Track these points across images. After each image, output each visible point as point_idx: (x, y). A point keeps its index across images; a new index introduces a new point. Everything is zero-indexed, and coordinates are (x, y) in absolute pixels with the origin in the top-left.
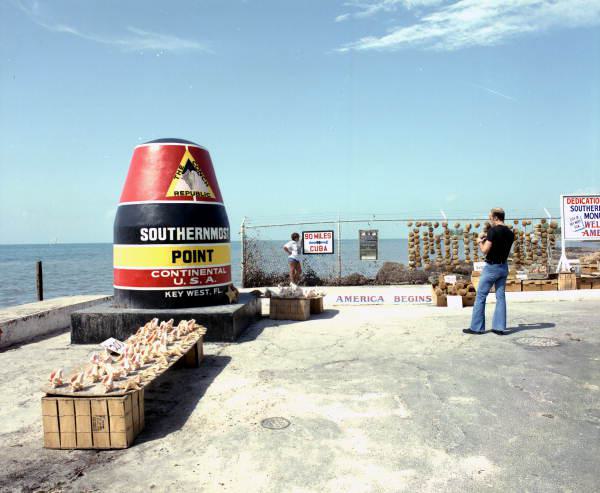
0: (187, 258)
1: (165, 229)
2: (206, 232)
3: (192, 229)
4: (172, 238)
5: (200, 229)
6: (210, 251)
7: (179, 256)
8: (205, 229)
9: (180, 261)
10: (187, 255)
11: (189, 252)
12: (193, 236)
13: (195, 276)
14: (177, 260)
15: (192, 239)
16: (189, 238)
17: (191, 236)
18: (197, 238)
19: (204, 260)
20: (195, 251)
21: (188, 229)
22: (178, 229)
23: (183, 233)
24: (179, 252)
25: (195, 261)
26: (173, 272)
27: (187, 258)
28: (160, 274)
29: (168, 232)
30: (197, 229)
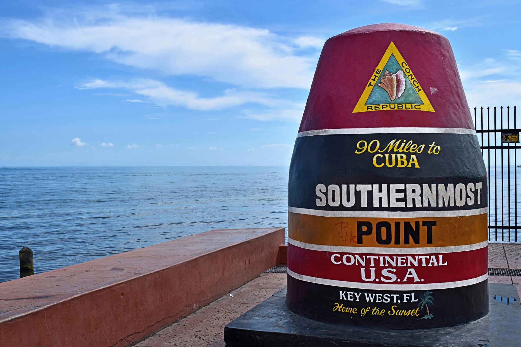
13: (390, 266)
26: (358, 257)
28: (340, 259)
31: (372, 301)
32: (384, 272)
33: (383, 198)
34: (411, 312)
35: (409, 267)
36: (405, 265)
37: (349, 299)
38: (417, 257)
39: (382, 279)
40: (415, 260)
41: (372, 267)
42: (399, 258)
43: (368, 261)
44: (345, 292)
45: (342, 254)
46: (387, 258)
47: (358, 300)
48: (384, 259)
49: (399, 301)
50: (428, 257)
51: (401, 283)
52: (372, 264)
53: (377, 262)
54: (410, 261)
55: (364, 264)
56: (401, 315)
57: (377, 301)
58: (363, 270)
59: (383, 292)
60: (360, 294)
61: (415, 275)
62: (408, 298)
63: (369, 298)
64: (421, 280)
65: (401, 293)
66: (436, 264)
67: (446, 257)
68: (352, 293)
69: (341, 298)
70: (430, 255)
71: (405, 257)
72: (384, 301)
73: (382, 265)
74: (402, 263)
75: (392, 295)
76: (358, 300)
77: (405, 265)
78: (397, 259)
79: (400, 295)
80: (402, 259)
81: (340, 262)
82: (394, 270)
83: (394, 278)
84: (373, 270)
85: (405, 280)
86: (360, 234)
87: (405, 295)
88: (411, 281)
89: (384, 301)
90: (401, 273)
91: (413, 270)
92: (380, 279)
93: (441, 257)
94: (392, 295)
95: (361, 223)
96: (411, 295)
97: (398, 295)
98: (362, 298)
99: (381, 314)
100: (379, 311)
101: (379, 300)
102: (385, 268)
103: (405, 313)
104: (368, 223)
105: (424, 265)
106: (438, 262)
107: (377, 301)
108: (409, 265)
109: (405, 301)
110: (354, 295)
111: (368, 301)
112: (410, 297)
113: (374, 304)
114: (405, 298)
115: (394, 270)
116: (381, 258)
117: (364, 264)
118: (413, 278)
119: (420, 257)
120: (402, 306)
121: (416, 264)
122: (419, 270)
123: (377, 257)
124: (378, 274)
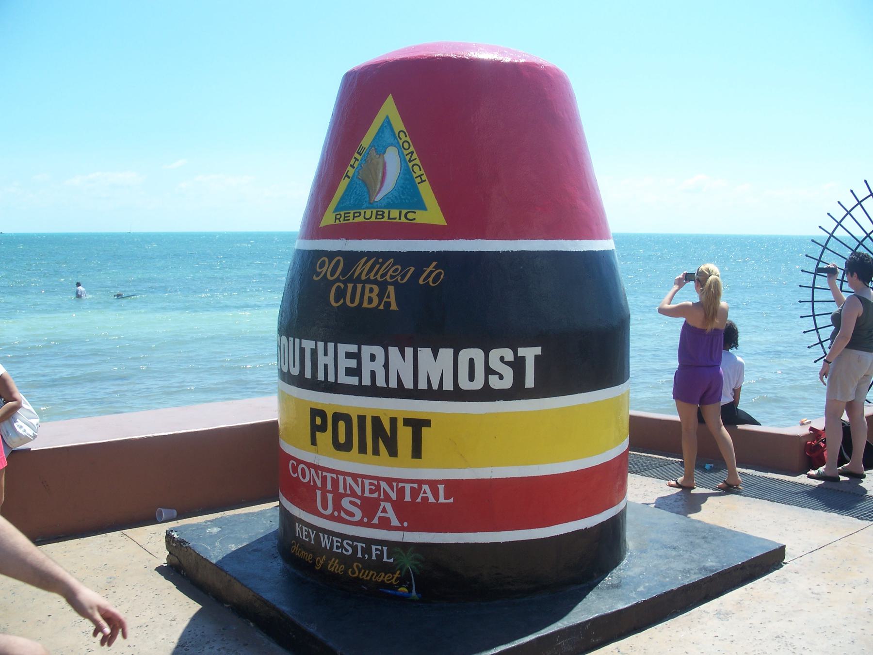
0: (342, 439)
1: (297, 340)
3: (353, 348)
4: (308, 375)
5: (378, 351)
6: (417, 425)
7: (323, 428)
8: (394, 351)
9: (325, 438)
10: (342, 425)
11: (347, 418)
13: (353, 494)
14: (318, 434)
15: (353, 381)
16: (343, 379)
17: (349, 372)
18: (366, 381)
19: (393, 452)
21: (343, 348)
23: (330, 360)
24: (322, 414)
25: (363, 450)
27: (342, 439)
29: (302, 350)
31: (328, 548)
32: (345, 503)
34: (384, 577)
35: (384, 500)
36: (375, 495)
37: (304, 538)
38: (395, 484)
39: (343, 514)
40: (393, 490)
41: (329, 492)
42: (367, 482)
43: (324, 479)
44: (300, 526)
45: (300, 462)
46: (349, 480)
47: (313, 542)
48: (345, 480)
49: (366, 556)
50: (416, 486)
51: (369, 525)
52: (329, 487)
53: (335, 482)
55: (319, 484)
56: (368, 578)
57: (335, 550)
58: (319, 493)
59: (343, 537)
60: (315, 532)
61: (391, 514)
62: (379, 553)
63: (325, 542)
64: (402, 524)
65: (369, 542)
66: (432, 500)
67: (452, 486)
68: (307, 529)
69: (297, 535)
70: (420, 482)
71: (375, 482)
72: (344, 551)
73: (341, 490)
74: (371, 491)
75: (355, 544)
76: (313, 542)
77: (375, 495)
78: (363, 483)
80: (370, 484)
81: (295, 475)
82: (359, 502)
83: (358, 515)
84: (330, 497)
85: (375, 521)
86: (315, 429)
87: (374, 547)
88: (385, 524)
89: (344, 551)
90: (369, 507)
91: (388, 506)
92: (339, 513)
93: (441, 488)
94: (355, 544)
95: (316, 412)
96: (382, 548)
97: (364, 545)
98: (317, 537)
100: (338, 565)
101: (338, 547)
102: (345, 495)
103: (374, 577)
105: (408, 498)
106: (436, 497)
107: (335, 550)
108: (382, 497)
109: (374, 558)
111: (323, 546)
112: (382, 551)
113: (330, 553)
114: (374, 553)
115: (359, 502)
116: (341, 478)
117: (319, 484)
118: (388, 520)
119: (400, 485)
120: (368, 565)
121: (393, 496)
122: (399, 506)
123: (334, 476)
124: (337, 506)
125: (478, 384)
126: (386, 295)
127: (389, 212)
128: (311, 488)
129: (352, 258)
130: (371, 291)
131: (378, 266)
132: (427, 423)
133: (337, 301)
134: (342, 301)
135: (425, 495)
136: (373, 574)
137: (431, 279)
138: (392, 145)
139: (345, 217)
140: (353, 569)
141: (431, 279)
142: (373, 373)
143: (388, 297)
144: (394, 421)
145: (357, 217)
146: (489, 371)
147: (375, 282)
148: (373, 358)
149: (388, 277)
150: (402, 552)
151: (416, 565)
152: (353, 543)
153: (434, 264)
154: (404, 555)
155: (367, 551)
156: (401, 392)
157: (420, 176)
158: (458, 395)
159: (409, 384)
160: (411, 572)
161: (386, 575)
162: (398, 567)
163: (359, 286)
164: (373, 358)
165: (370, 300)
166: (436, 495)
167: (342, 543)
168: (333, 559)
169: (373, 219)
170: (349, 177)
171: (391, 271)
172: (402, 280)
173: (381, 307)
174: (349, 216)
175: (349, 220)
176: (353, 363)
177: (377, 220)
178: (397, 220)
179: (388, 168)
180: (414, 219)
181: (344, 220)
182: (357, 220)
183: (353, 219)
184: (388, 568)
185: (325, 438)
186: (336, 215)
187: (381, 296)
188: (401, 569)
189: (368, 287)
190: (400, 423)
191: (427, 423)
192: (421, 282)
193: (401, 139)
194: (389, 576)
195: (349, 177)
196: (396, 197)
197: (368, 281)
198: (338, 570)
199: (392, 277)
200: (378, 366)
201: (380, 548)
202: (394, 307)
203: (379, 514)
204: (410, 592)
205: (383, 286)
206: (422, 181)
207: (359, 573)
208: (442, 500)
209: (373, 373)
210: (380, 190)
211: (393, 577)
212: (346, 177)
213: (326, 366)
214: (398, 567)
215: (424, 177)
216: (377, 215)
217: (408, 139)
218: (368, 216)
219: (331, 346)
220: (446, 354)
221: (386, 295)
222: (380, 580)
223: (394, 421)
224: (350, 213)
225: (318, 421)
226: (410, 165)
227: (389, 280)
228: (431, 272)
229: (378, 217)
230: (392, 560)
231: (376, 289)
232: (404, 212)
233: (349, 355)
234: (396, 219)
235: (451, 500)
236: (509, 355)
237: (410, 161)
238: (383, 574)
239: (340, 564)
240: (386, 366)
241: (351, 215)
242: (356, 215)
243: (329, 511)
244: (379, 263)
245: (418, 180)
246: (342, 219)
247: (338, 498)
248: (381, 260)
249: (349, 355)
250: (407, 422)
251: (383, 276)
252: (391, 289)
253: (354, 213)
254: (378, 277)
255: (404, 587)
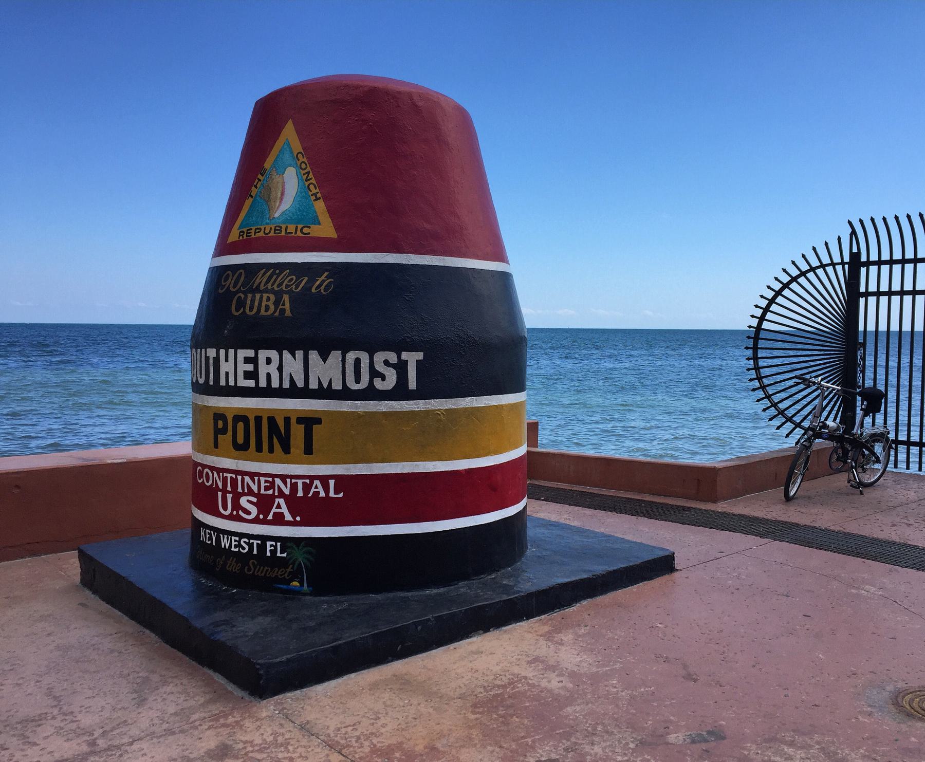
2: (293, 365)
3: (250, 353)
5: (273, 354)
6: (309, 422)
7: (224, 431)
8: (286, 355)
9: (226, 440)
10: (241, 425)
12: (252, 375)
13: (251, 492)
15: (251, 383)
17: (248, 375)
19: (286, 449)
20: (258, 419)
21: (243, 353)
22: (222, 352)
25: (259, 449)
27: (240, 440)
30: (263, 354)
31: (227, 548)
32: (243, 501)
33: (243, 378)
34: (277, 573)
35: (279, 497)
36: (270, 492)
38: (288, 480)
41: (229, 492)
43: (225, 479)
45: (204, 466)
46: (247, 479)
50: (308, 481)
51: (265, 522)
52: (229, 488)
53: (234, 482)
54: (278, 485)
55: (220, 485)
56: (263, 574)
57: (233, 549)
58: (220, 494)
59: (241, 535)
60: (216, 534)
61: (284, 510)
62: (273, 548)
63: (225, 543)
64: (294, 517)
65: (264, 538)
66: (322, 494)
68: (210, 532)
69: (202, 539)
70: (312, 478)
71: (270, 479)
73: (240, 490)
74: (266, 489)
75: (251, 541)
77: (270, 492)
78: (259, 480)
79: (279, 542)
83: (254, 510)
84: (229, 496)
85: (270, 517)
86: (218, 432)
87: (269, 543)
88: (279, 520)
90: (264, 503)
91: (282, 501)
92: (238, 512)
93: (332, 483)
94: (251, 541)
96: (276, 544)
97: (259, 542)
99: (236, 570)
102: (244, 494)
104: (219, 416)
105: (300, 494)
106: (327, 490)
107: (233, 549)
108: (276, 494)
110: (210, 534)
112: (276, 547)
114: (269, 548)
115: (254, 500)
116: (239, 478)
117: (220, 485)
118: (282, 514)
119: (293, 481)
121: (287, 491)
122: (291, 500)
123: (234, 476)
125: (364, 383)
126: (282, 303)
127: (287, 227)
128: (214, 490)
129: (251, 270)
130: (268, 299)
131: (275, 277)
132: (318, 421)
133: (237, 310)
134: (242, 310)
135: (316, 490)
136: (267, 570)
137: (323, 288)
138: (290, 166)
139: (247, 233)
140: (249, 566)
141: (323, 288)
142: (269, 376)
143: (284, 304)
144: (287, 420)
145: (257, 233)
146: (375, 373)
147: (272, 291)
148: (269, 361)
149: (283, 287)
150: (294, 546)
151: (308, 560)
152: (249, 541)
153: (326, 274)
154: (296, 549)
155: (262, 547)
156: (293, 392)
157: (315, 194)
158: (346, 394)
159: (300, 384)
160: (303, 566)
161: (279, 570)
162: (291, 561)
163: (258, 296)
164: (269, 361)
165: (267, 308)
166: (326, 489)
167: (239, 541)
168: (231, 558)
169: (272, 234)
170: (252, 197)
171: (286, 280)
172: (296, 288)
173: (277, 314)
174: (251, 232)
175: (251, 236)
176: (250, 367)
177: (275, 235)
178: (293, 235)
179: (287, 186)
180: (309, 233)
181: (247, 236)
182: (257, 235)
183: (255, 235)
184: (283, 562)
185: (226, 440)
186: (240, 232)
187: (276, 303)
188: (293, 563)
189: (265, 295)
190: (293, 421)
191: (318, 421)
192: (313, 290)
193: (299, 160)
194: (282, 571)
195: (252, 197)
196: (293, 213)
197: (266, 291)
198: (235, 569)
199: (287, 286)
200: (273, 369)
201: (274, 543)
202: (288, 313)
203: (274, 510)
204: (302, 585)
205: (279, 295)
206: (317, 199)
207: (255, 570)
208: (332, 494)
209: (269, 376)
210: (279, 206)
211: (286, 571)
212: (250, 198)
213: (227, 373)
214: (291, 561)
215: (319, 195)
216: (275, 230)
217: (305, 160)
218: (267, 231)
219: (231, 352)
220: (336, 356)
221: (282, 303)
222: (274, 576)
223: (287, 420)
224: (251, 229)
225: (220, 424)
226: (307, 184)
227: (284, 289)
228: (323, 281)
229: (277, 232)
230: (285, 555)
231: (272, 297)
232: (300, 226)
233: (247, 360)
234: (292, 233)
235: (341, 495)
236: (392, 357)
237: (307, 180)
238: (277, 569)
239: (237, 562)
240: (280, 369)
241: (253, 231)
242: (257, 230)
243: (227, 513)
244: (276, 274)
245: (314, 198)
246: (245, 235)
247: (237, 497)
248: (277, 272)
249: (247, 360)
250: (300, 420)
251: (279, 285)
252: (286, 298)
253: (256, 229)
254: (275, 287)
255: (296, 581)
